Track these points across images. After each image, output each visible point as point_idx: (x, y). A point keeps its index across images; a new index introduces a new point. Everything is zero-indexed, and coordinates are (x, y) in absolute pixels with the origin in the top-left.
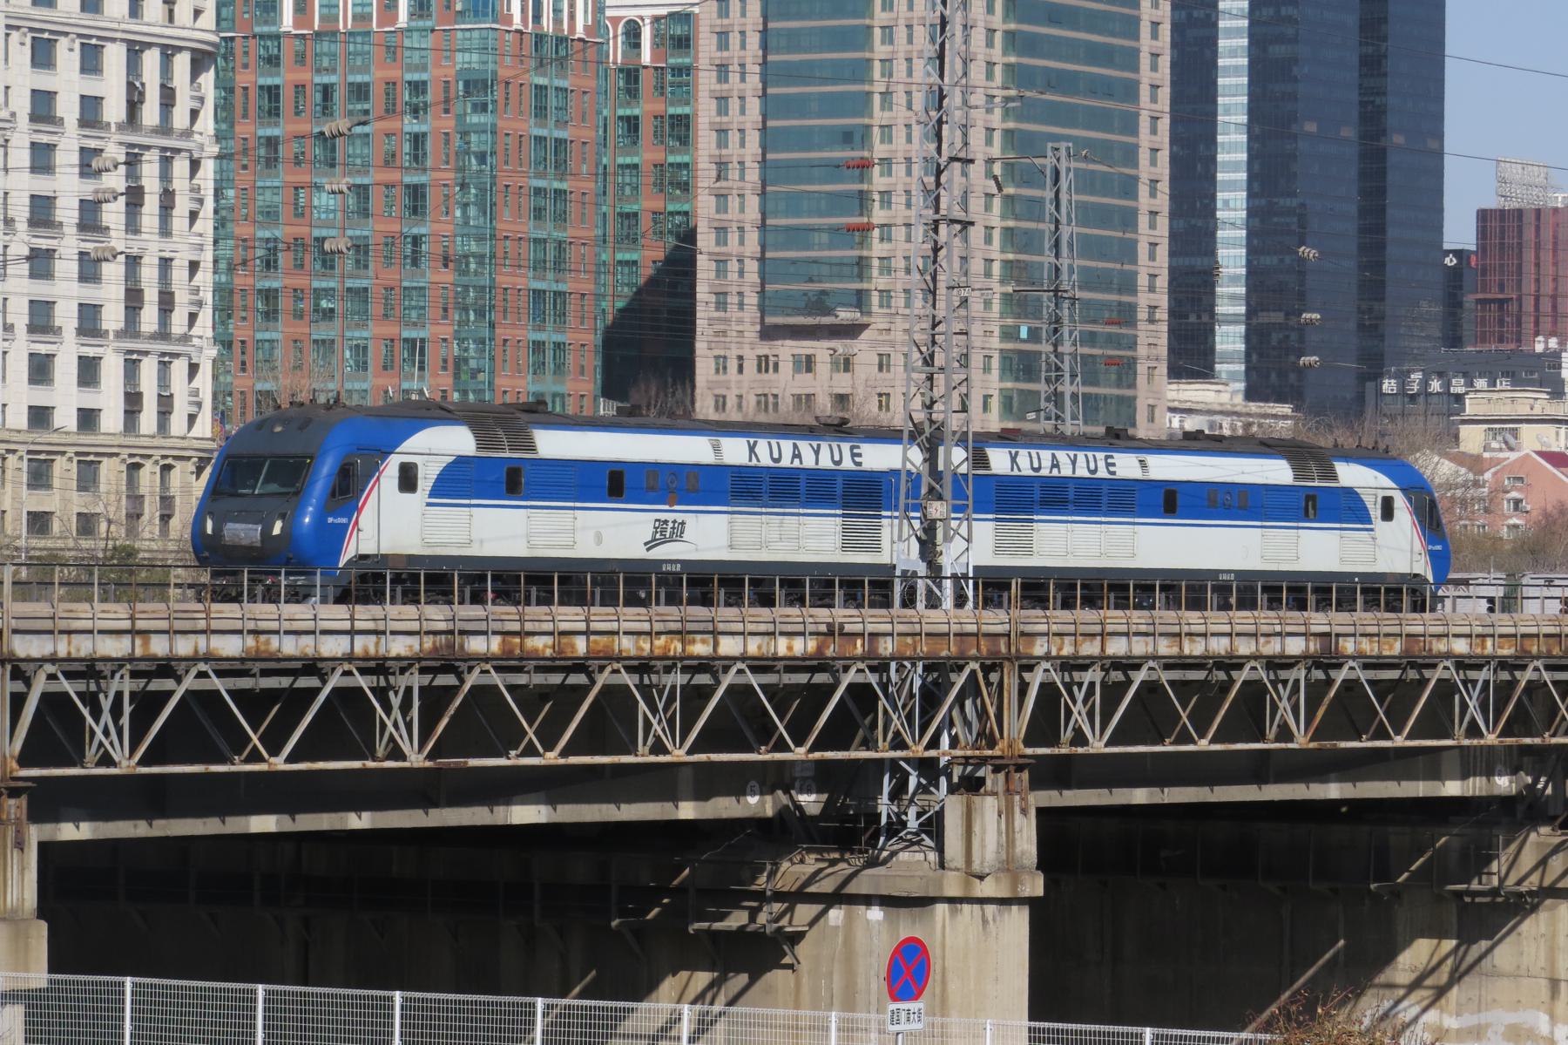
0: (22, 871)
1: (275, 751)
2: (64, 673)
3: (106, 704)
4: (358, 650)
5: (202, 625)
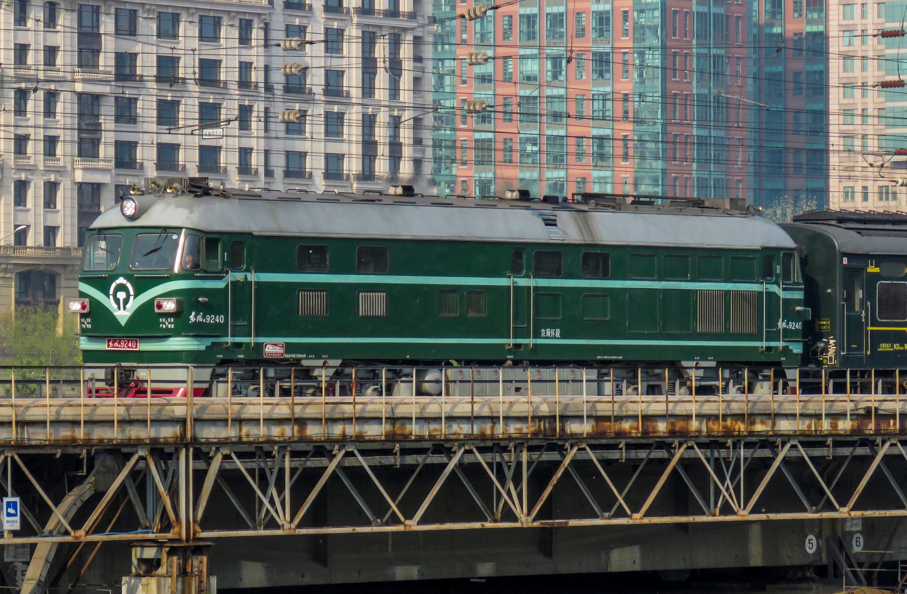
1: (409, 516)
2: (236, 453)
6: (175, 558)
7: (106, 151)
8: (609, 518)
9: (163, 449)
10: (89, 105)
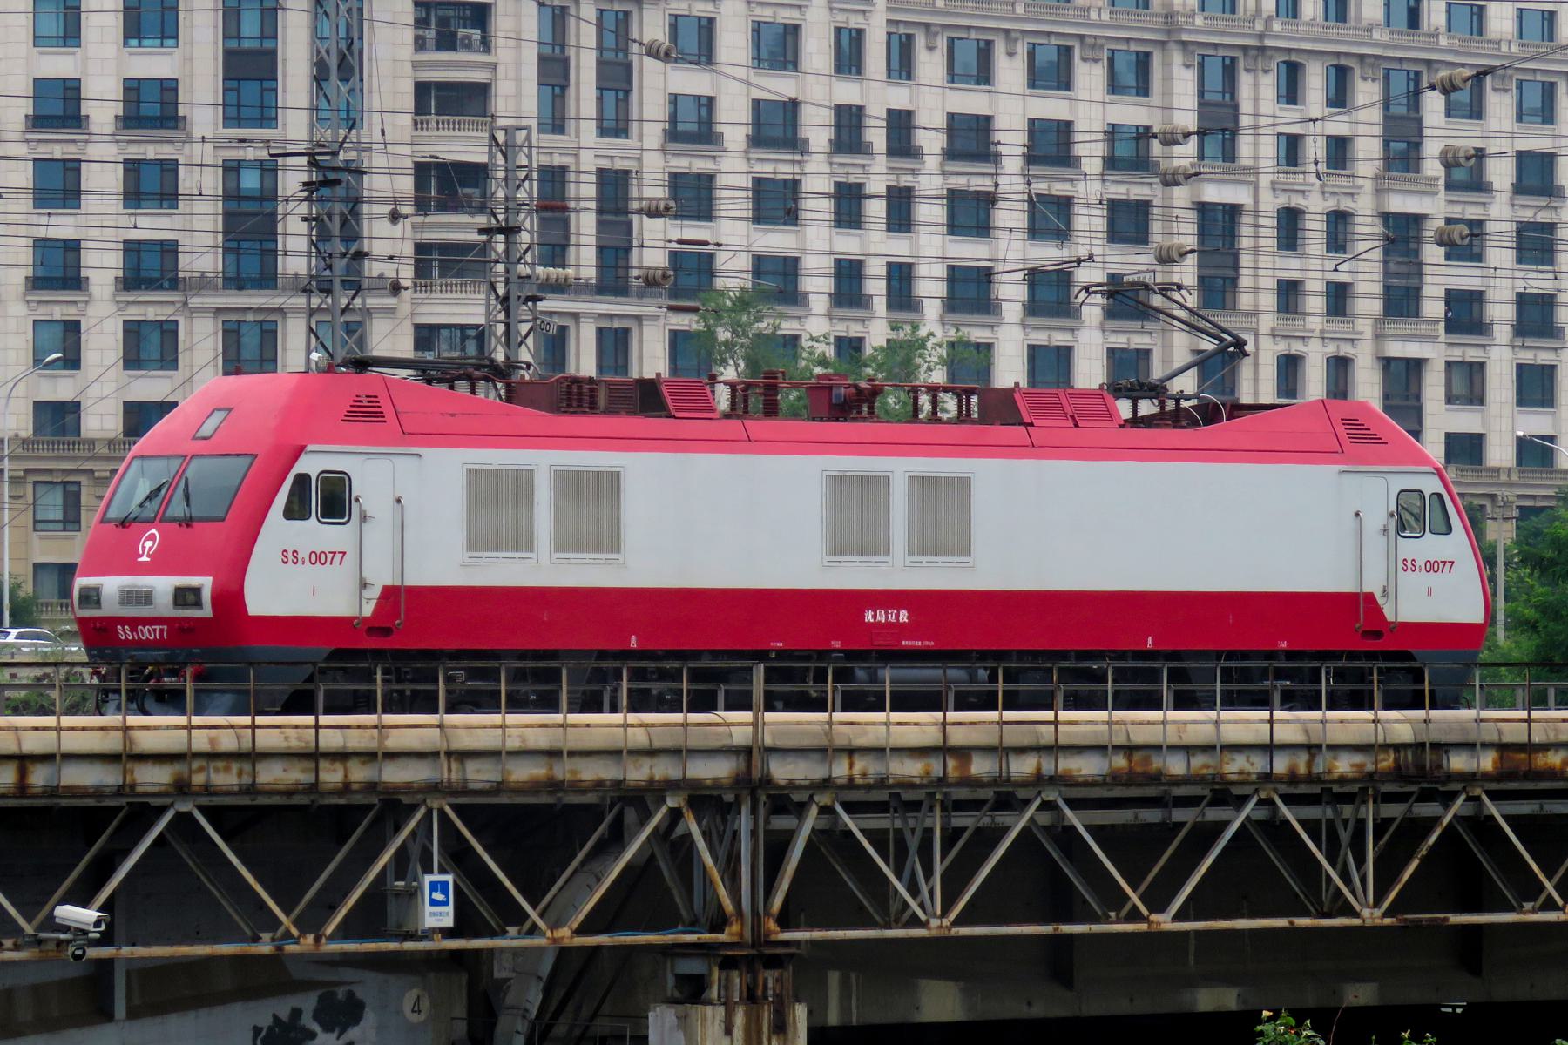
1: (1160, 907)
3: (913, 843)
4: (1281, 765)
7: (1434, 308)
8: (1534, 911)
9: (720, 797)
10: (1402, 233)
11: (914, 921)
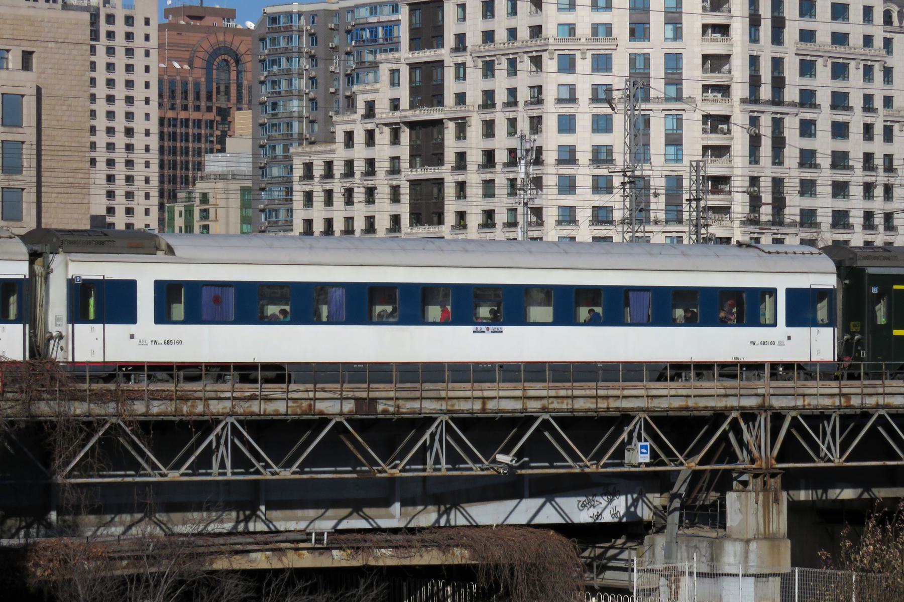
0: (779, 513)
3: (829, 430)
5: (880, 390)
6: (759, 481)
11: (829, 460)
